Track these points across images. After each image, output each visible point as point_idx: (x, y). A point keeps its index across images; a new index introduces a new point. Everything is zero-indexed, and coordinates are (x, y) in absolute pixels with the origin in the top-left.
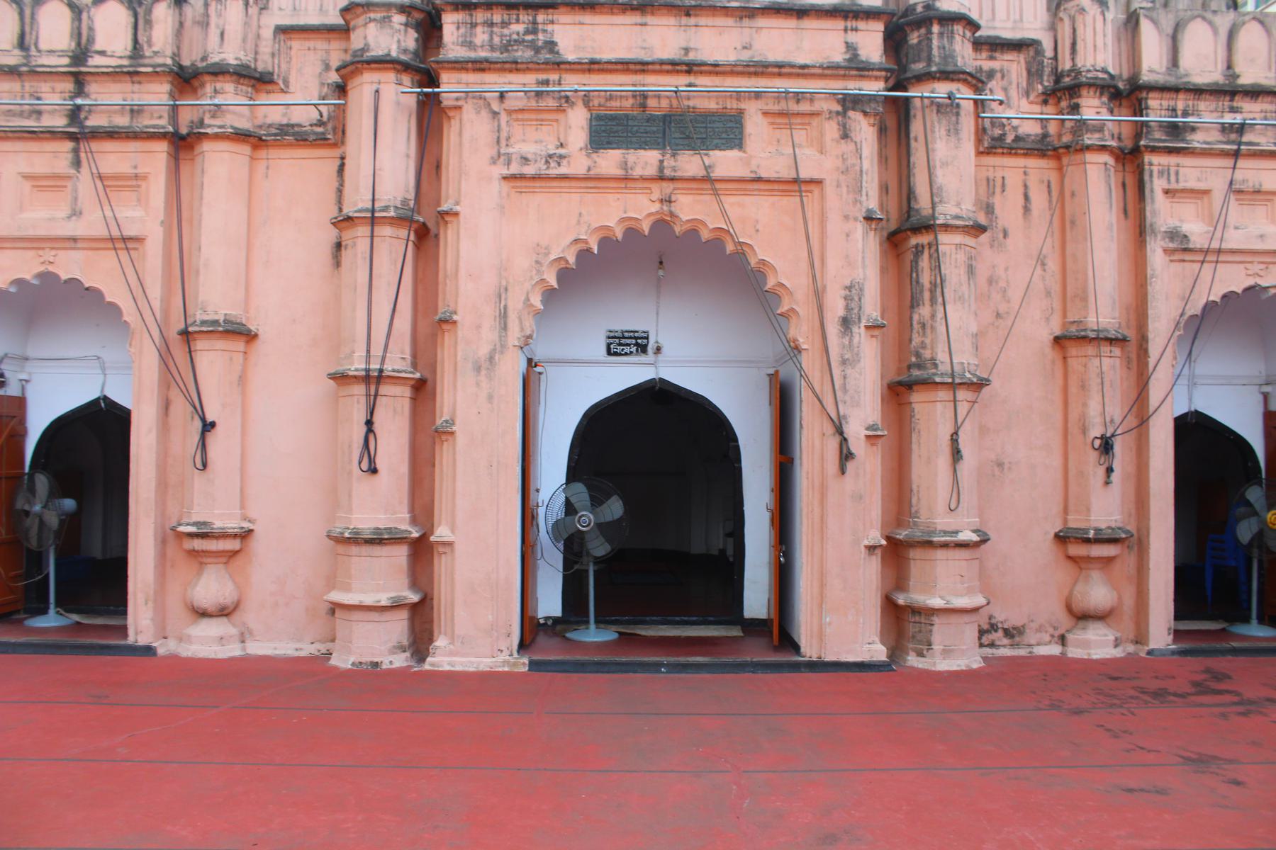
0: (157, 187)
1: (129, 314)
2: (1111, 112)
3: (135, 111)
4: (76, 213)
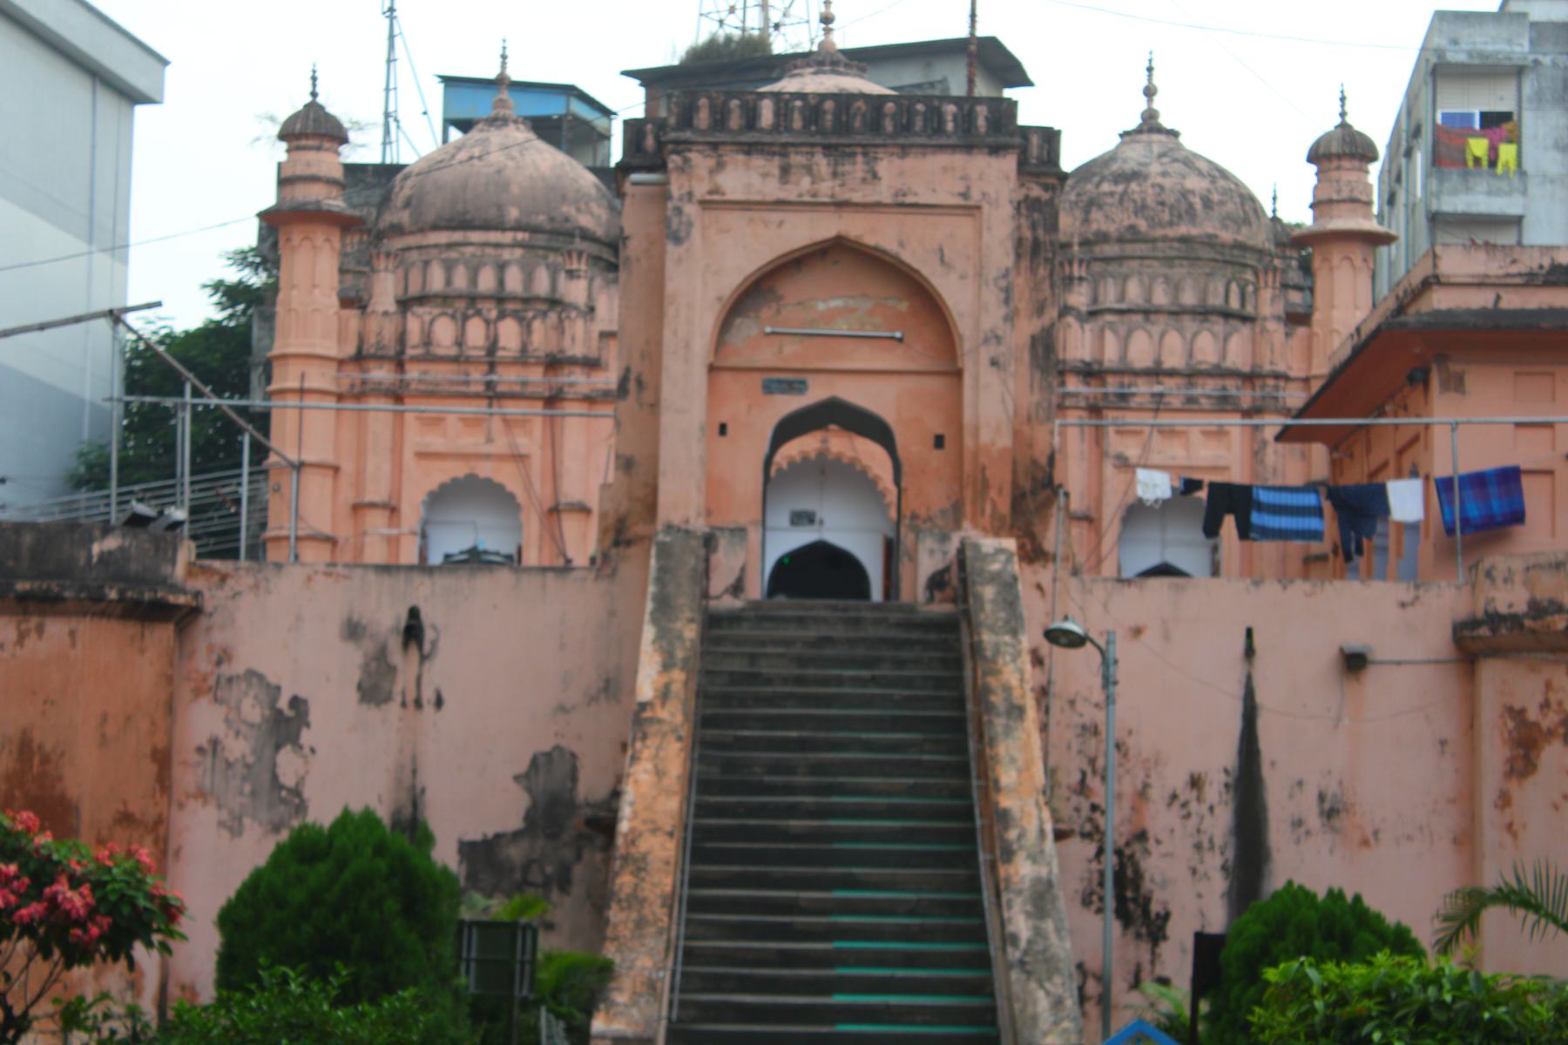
0: (537, 426)
1: (521, 496)
2: (1088, 384)
3: (524, 384)
4: (489, 440)
